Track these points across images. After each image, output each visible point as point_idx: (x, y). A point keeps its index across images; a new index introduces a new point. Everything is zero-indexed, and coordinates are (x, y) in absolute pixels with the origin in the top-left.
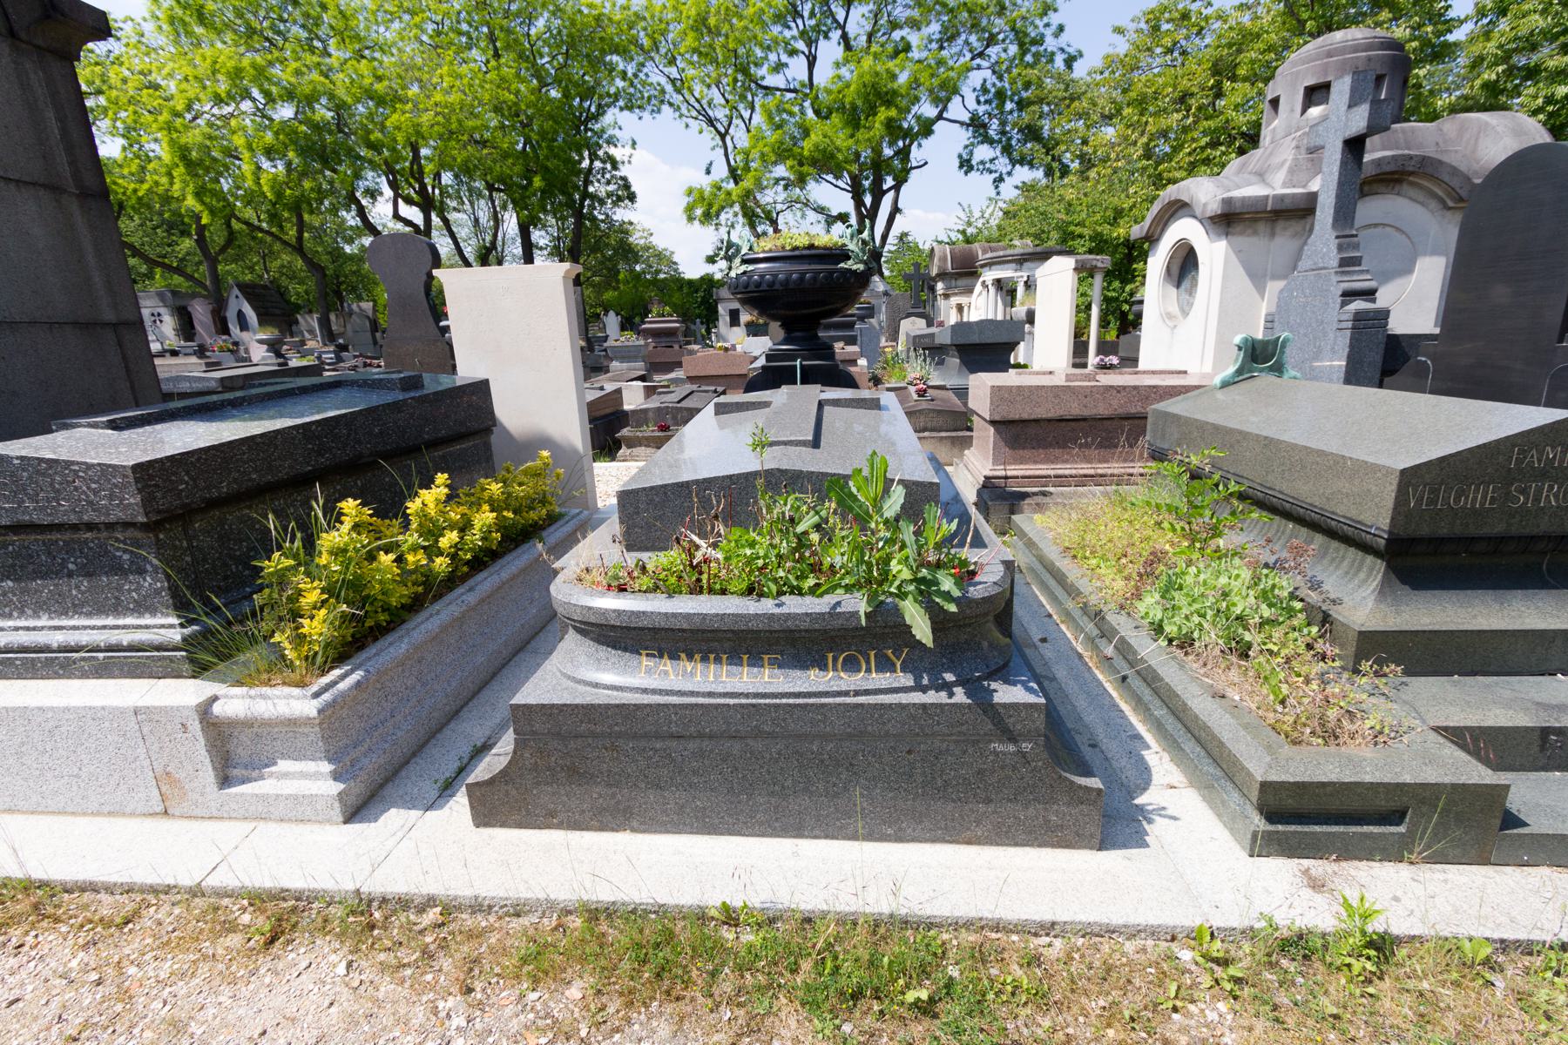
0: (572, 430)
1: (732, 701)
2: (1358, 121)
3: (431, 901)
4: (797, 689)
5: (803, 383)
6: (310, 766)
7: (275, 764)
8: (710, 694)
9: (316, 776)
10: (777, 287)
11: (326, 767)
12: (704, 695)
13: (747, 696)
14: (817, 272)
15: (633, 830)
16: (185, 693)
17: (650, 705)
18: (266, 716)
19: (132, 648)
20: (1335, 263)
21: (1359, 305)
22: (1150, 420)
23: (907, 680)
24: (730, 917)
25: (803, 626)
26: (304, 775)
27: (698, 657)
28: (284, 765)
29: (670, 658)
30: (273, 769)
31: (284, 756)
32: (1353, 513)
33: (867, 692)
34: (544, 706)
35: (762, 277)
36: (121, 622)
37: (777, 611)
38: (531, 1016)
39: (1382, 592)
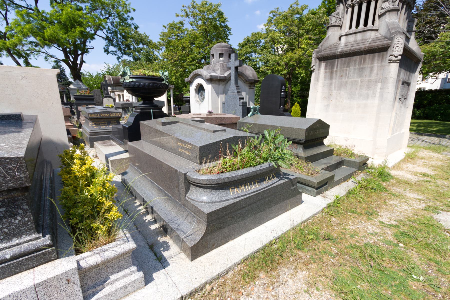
0: (64, 138)
1: (254, 194)
2: (237, 63)
3: (205, 284)
4: (264, 187)
5: (153, 119)
6: (127, 271)
7: (109, 278)
8: (250, 194)
9: (133, 272)
10: (145, 87)
11: (134, 268)
12: (243, 196)
13: (256, 191)
14: (154, 84)
15: (232, 239)
16: (65, 265)
17: (238, 201)
18: (113, 256)
19: (14, 258)
20: (236, 92)
21: (242, 101)
22: (238, 124)
23: (276, 179)
24: (271, 243)
25: (265, 171)
26: (125, 276)
27: (243, 186)
28: (113, 277)
29: (237, 188)
30: (109, 281)
31: (112, 274)
32: (297, 137)
33: (274, 183)
34: (215, 211)
35: (135, 83)
36: (22, 240)
37: (261, 168)
38: (262, 287)
39: (303, 151)
